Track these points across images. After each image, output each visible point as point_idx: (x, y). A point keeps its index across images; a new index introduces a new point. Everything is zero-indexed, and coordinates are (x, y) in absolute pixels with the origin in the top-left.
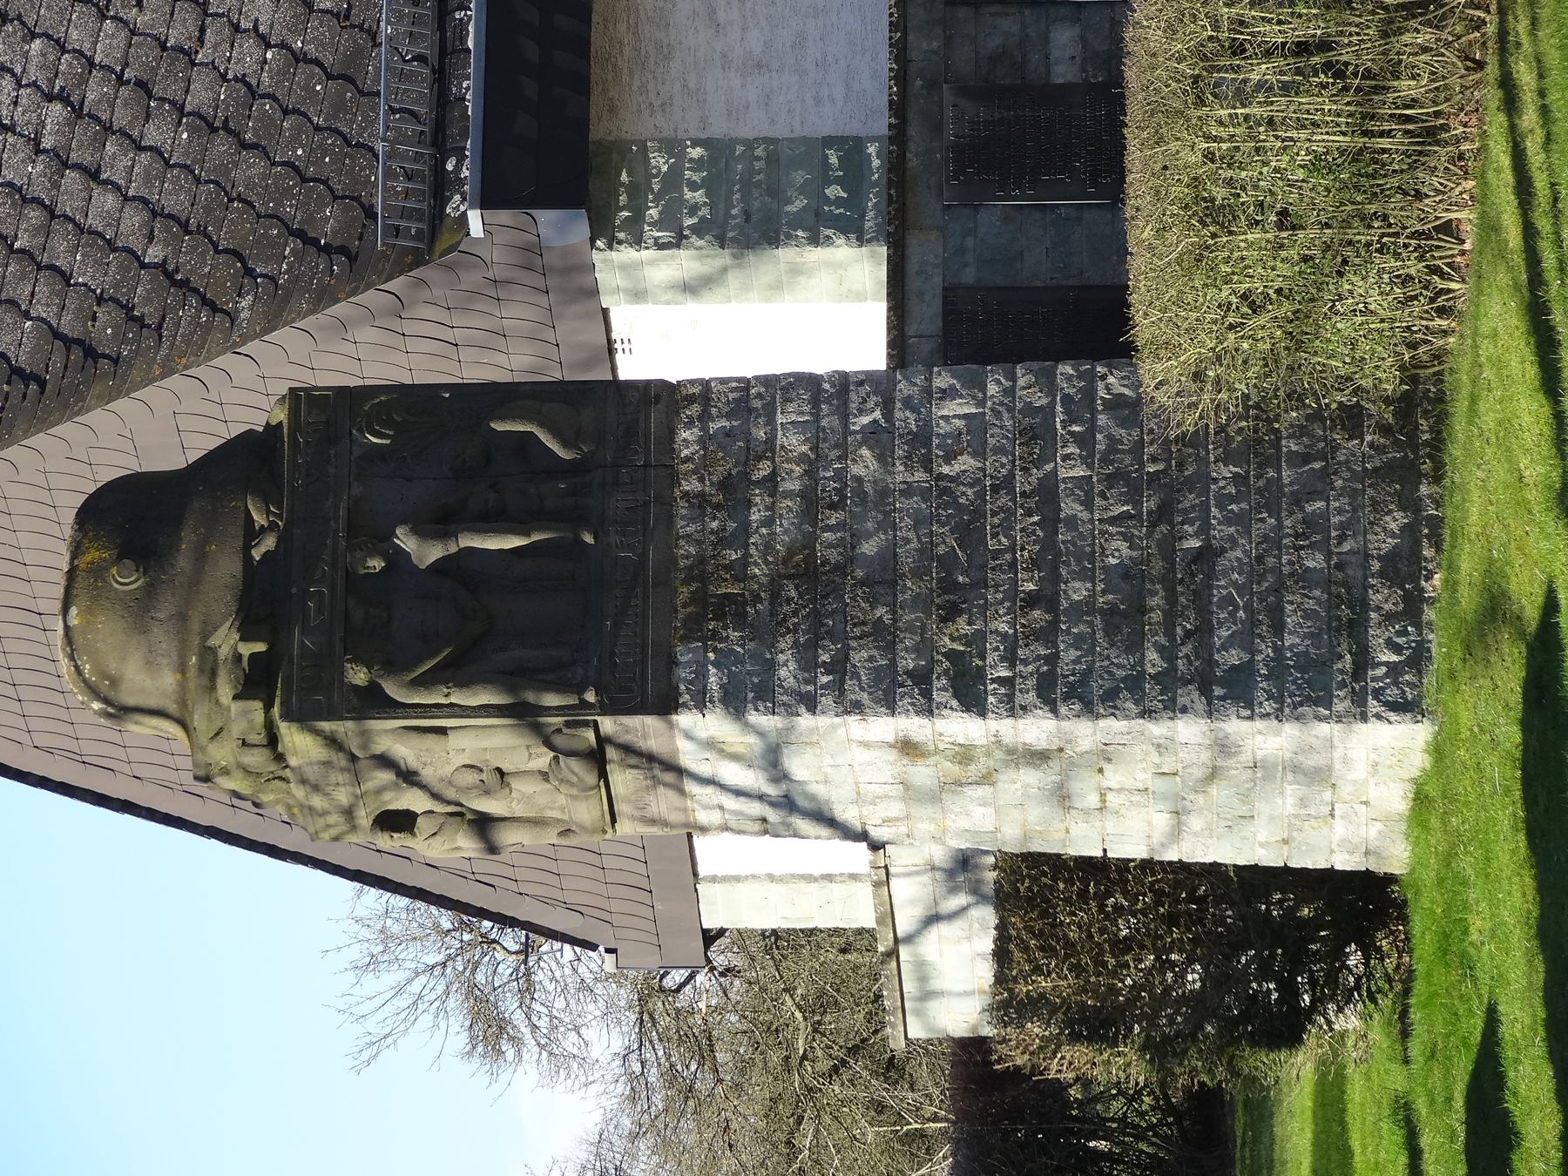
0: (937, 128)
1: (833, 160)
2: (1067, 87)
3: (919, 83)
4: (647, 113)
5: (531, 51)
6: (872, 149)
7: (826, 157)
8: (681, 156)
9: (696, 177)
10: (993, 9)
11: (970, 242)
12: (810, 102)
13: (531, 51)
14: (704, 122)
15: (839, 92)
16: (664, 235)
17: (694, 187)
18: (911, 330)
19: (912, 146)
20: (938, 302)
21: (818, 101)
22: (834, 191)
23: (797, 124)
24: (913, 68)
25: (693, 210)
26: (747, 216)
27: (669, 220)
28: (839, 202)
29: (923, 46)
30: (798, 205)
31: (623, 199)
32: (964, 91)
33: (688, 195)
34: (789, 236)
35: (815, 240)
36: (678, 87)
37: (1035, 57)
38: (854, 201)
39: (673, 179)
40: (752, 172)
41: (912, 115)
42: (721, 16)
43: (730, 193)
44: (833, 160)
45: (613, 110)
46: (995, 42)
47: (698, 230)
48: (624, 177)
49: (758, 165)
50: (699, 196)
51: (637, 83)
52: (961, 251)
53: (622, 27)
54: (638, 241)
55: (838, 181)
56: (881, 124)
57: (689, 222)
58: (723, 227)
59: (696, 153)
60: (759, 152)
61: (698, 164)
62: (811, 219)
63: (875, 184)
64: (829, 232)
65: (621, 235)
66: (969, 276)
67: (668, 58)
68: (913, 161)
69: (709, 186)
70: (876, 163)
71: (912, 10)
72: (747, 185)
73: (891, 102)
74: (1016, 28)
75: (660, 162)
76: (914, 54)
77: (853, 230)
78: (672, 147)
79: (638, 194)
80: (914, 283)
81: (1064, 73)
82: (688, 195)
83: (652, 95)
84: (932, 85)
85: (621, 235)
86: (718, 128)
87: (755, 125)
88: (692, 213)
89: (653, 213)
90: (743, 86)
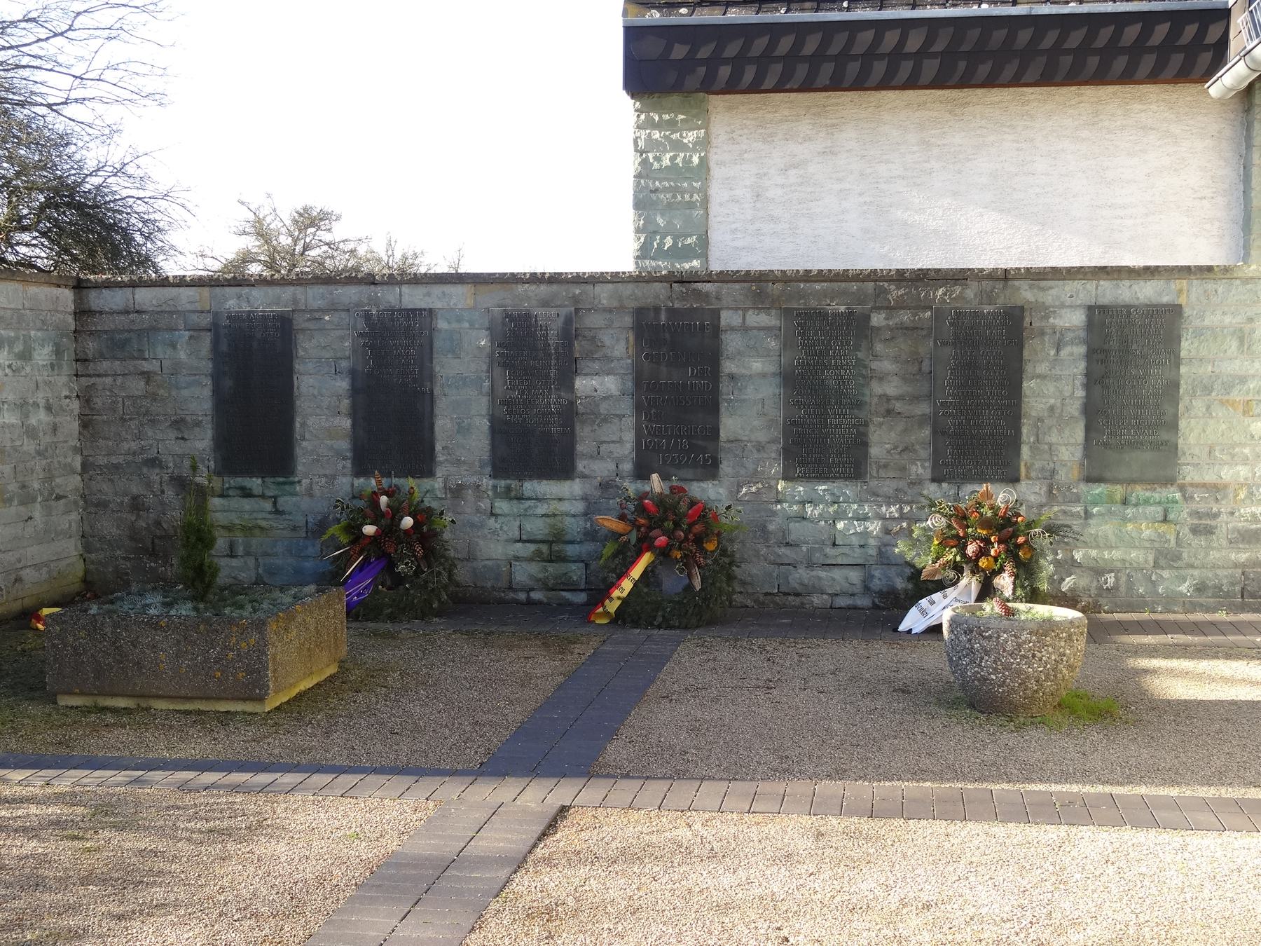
0: (545, 303)
1: (689, 241)
2: (571, 388)
3: (577, 292)
4: (728, 129)
5: (705, 52)
6: (696, 263)
7: (691, 236)
8: (694, 150)
9: (679, 160)
10: (631, 339)
11: (466, 325)
12: (734, 226)
13: (705, 52)
14: (721, 163)
15: (739, 244)
16: (641, 144)
17: (673, 159)
18: (405, 289)
19: (533, 287)
20: (423, 306)
21: (734, 231)
22: (669, 242)
23: (719, 219)
24: (589, 287)
25: (658, 159)
26: (656, 191)
27: (652, 144)
28: (662, 244)
29: (603, 294)
30: (660, 221)
31: (666, 117)
32: (568, 321)
33: (668, 156)
34: (640, 216)
35: (638, 231)
36: (745, 147)
37: (596, 366)
38: (661, 254)
39: (678, 146)
40: (683, 193)
41: (555, 287)
42: (792, 172)
43: (669, 180)
44: (689, 241)
45: (730, 109)
46: (607, 340)
47: (644, 163)
48: (681, 117)
49: (687, 197)
50: (666, 161)
51: (748, 123)
52: (459, 320)
53: (786, 113)
54: (639, 127)
55: (675, 244)
56: (716, 267)
57: (651, 156)
58: (647, 177)
59: (696, 160)
60: (696, 197)
61: (687, 161)
62: (651, 228)
63: (672, 265)
64: (642, 240)
65: (643, 117)
66: (442, 324)
67: (764, 141)
68: (521, 289)
69: (674, 166)
70: (687, 266)
71: (631, 287)
72: (674, 190)
73: (561, 274)
74: (617, 354)
75: (690, 137)
76: (598, 288)
77: (644, 252)
78: (704, 144)
79: (672, 125)
80: (437, 290)
81: (583, 384)
82: (668, 156)
83: (740, 132)
84: (576, 300)
85: (643, 117)
86: (717, 172)
87: (718, 194)
88: (656, 158)
89: (656, 135)
90: (745, 187)
